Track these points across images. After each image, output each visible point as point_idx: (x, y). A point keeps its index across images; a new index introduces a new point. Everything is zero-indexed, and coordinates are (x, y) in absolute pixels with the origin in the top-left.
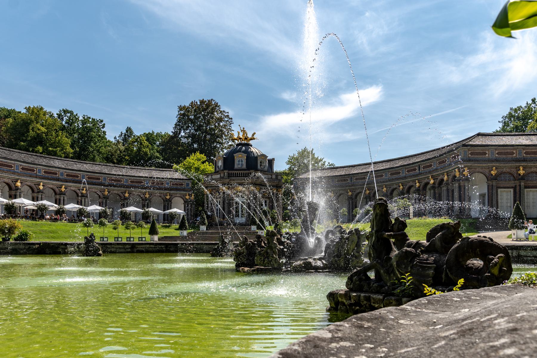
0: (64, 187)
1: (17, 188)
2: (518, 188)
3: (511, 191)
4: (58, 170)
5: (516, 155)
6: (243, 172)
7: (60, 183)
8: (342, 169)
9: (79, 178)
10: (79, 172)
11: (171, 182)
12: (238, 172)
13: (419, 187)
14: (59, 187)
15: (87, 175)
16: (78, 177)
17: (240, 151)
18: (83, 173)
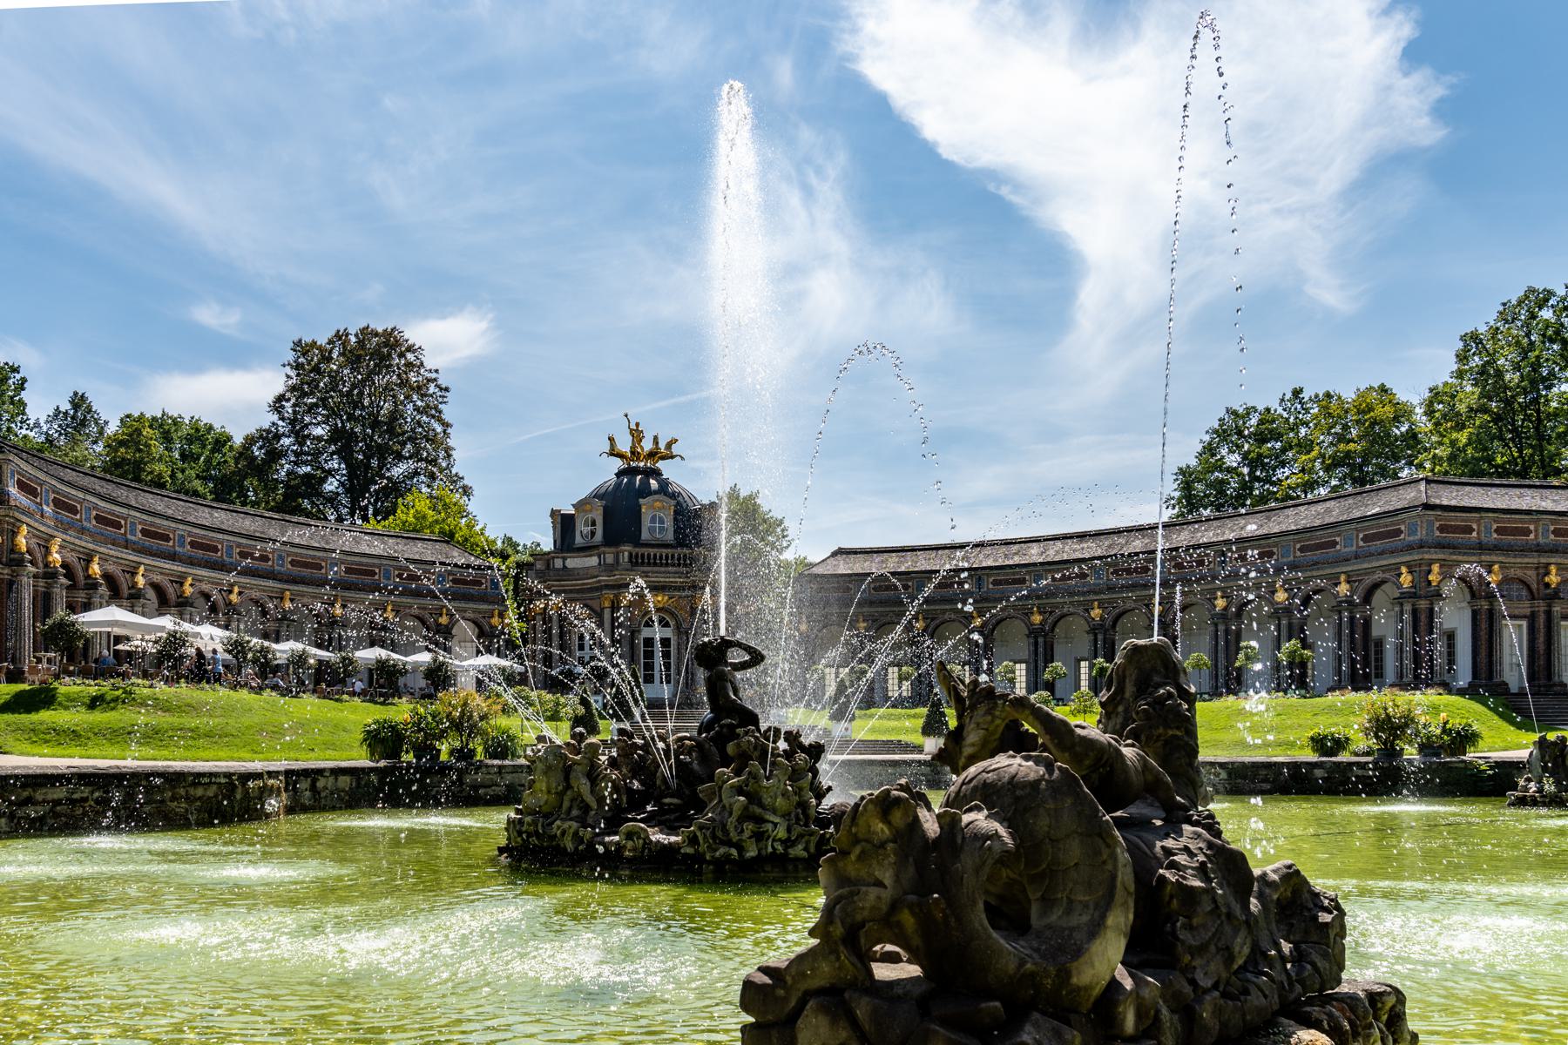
0: (190, 580)
1: (92, 585)
2: (1542, 619)
3: (1520, 626)
4: (173, 525)
5: (1357, 536)
6: (664, 551)
7: (180, 569)
8: (933, 554)
9: (219, 554)
10: (220, 536)
11: (450, 573)
12: (652, 551)
13: (1225, 609)
14: (176, 582)
15: (239, 545)
16: (215, 550)
17: (645, 491)
18: (230, 538)
